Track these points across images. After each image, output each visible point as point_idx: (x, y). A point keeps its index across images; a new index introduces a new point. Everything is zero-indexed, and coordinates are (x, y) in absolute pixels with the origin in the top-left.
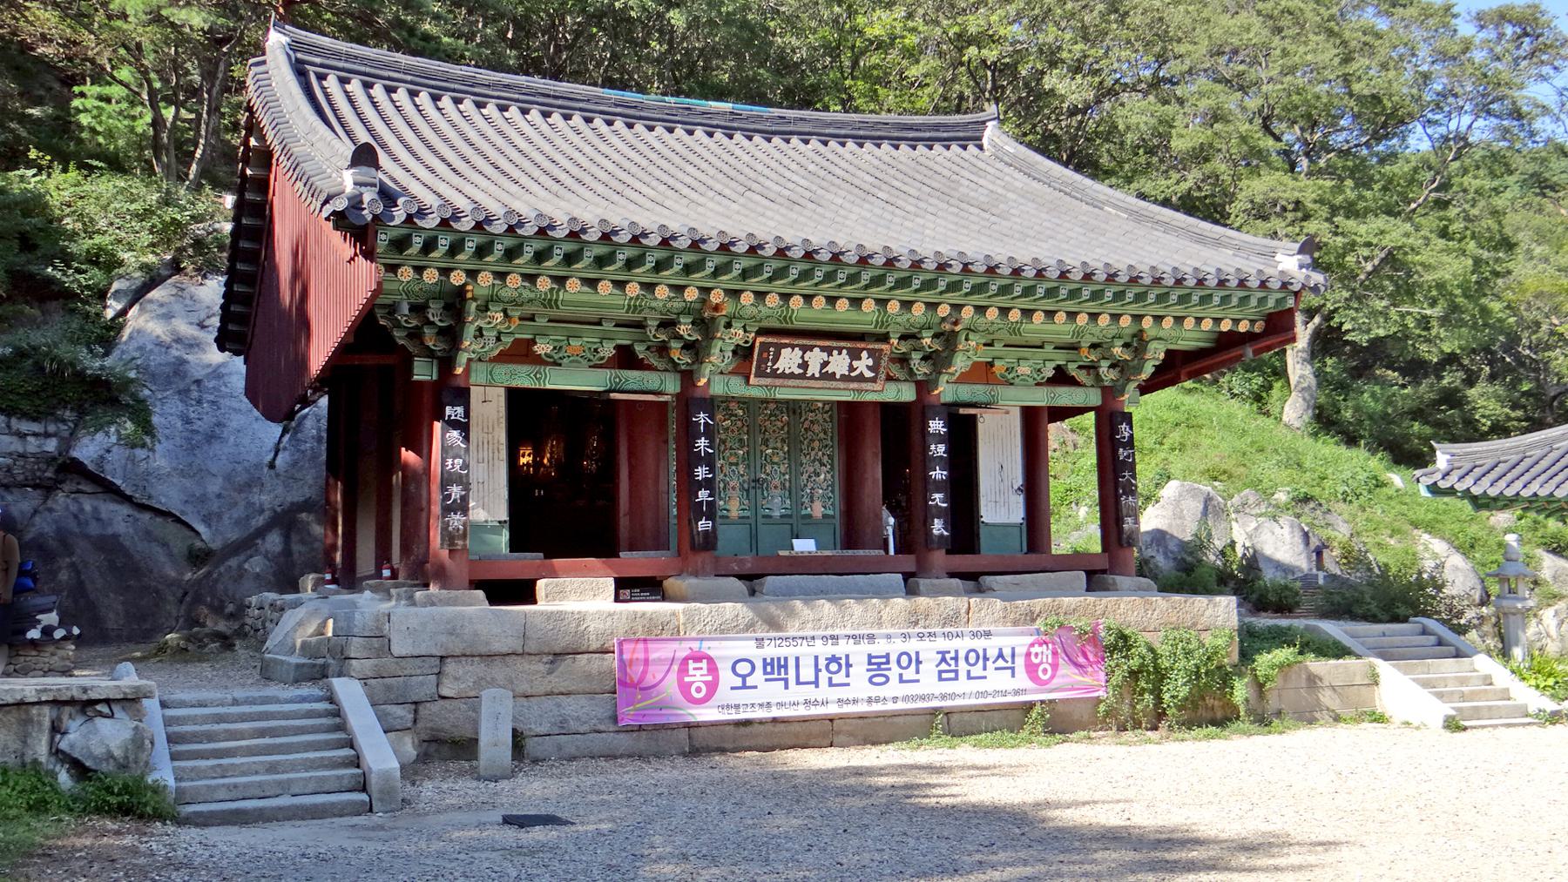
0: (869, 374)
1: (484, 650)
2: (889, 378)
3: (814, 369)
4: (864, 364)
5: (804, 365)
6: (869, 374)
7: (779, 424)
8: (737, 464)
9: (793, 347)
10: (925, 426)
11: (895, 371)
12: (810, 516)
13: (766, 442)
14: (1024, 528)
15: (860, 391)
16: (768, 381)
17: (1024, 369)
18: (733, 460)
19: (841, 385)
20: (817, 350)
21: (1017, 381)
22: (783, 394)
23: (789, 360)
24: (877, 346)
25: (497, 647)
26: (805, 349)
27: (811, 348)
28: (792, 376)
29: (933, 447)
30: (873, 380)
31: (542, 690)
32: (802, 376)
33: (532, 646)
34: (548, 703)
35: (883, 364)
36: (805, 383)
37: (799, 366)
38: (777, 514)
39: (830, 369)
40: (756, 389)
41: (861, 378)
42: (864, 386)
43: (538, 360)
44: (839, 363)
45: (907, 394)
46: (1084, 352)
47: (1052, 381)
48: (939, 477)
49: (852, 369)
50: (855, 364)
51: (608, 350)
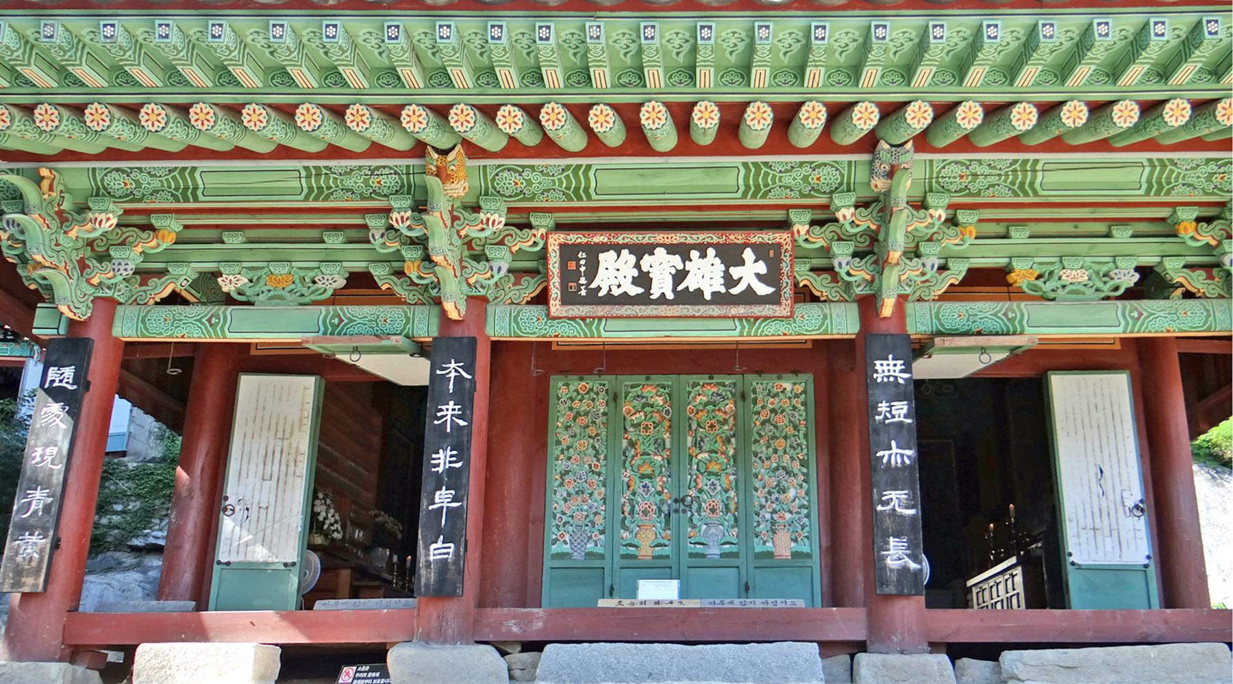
0: (763, 290)
2: (805, 295)
3: (662, 285)
4: (750, 272)
5: (643, 279)
6: (763, 290)
7: (721, 416)
8: (650, 477)
9: (618, 249)
10: (870, 369)
11: (820, 285)
12: (770, 555)
13: (698, 444)
14: (1153, 572)
16: (584, 310)
17: (1075, 274)
18: (647, 470)
19: (715, 310)
20: (660, 252)
24: (767, 237)
26: (640, 251)
27: (650, 249)
28: (625, 299)
29: (883, 407)
30: (774, 299)
32: (644, 299)
35: (785, 268)
37: (635, 282)
38: (714, 551)
39: (691, 283)
41: (749, 297)
42: (757, 310)
44: (706, 274)
45: (843, 323)
46: (1187, 230)
47: (1132, 294)
48: (896, 461)
49: (730, 281)
50: (735, 272)
51: (334, 279)
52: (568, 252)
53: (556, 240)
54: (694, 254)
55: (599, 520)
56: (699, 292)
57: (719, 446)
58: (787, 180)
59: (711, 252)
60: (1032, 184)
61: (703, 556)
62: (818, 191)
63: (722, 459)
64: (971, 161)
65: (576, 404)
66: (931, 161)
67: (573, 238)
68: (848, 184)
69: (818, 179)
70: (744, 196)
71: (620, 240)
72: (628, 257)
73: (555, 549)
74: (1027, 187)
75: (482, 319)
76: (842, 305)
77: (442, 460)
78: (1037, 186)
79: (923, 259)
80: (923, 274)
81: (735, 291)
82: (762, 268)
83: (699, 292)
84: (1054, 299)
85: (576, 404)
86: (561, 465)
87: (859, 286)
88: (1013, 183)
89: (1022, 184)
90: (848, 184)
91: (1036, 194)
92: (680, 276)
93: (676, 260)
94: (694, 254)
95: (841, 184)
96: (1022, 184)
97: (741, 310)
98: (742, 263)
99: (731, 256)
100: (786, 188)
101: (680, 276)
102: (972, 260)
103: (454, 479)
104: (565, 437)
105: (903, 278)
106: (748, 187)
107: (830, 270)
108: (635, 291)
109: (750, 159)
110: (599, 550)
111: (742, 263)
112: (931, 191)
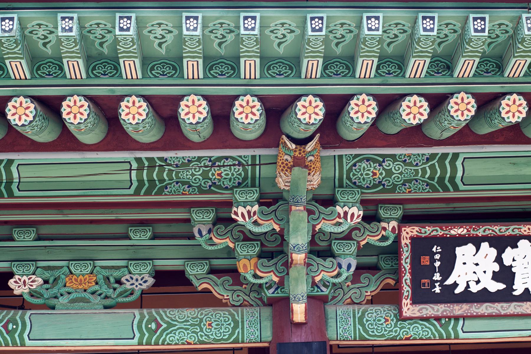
58: (185, 175)
60: (452, 179)
62: (219, 187)
64: (384, 156)
66: (340, 157)
68: (253, 178)
69: (219, 175)
70: (137, 193)
74: (446, 181)
76: (256, 311)
78: (458, 180)
79: (340, 260)
80: (339, 275)
87: (269, 288)
88: (431, 178)
89: (441, 180)
90: (253, 178)
91: (456, 189)
95: (245, 178)
96: (441, 180)
100: (184, 183)
102: (158, 262)
105: (317, 279)
106: (141, 182)
107: (233, 272)
109: (144, 155)
112: (341, 186)
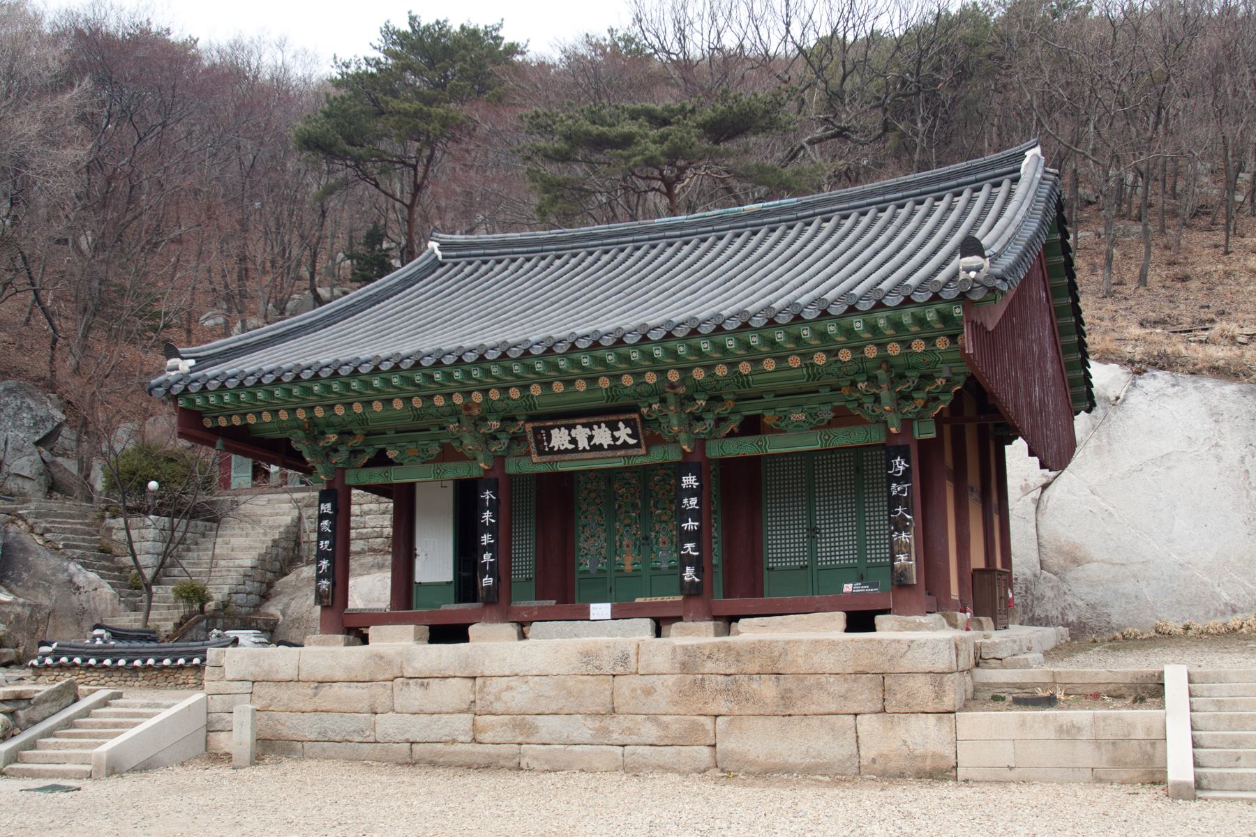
0: (632, 441)
1: (276, 678)
3: (583, 444)
4: (624, 433)
5: (573, 441)
6: (632, 441)
8: (629, 525)
15: (629, 457)
16: (549, 458)
19: (610, 454)
20: (579, 427)
21: (790, 427)
22: (562, 468)
23: (560, 439)
25: (281, 676)
26: (570, 428)
28: (566, 451)
29: (685, 501)
30: (637, 446)
31: (311, 708)
33: (303, 676)
34: (315, 717)
36: (579, 456)
37: (570, 442)
38: (665, 566)
39: (596, 441)
40: (534, 464)
41: (625, 445)
42: (630, 452)
43: (390, 463)
44: (603, 436)
49: (615, 439)
50: (616, 434)
52: (536, 431)
53: (529, 427)
54: (595, 427)
55: (603, 551)
56: (601, 445)
57: (667, 506)
59: (603, 425)
61: (659, 569)
63: (669, 513)
65: (589, 486)
67: (537, 424)
71: (559, 423)
72: (564, 431)
73: (582, 568)
75: (503, 466)
77: (486, 539)
81: (618, 443)
82: (629, 431)
83: (601, 445)
84: (781, 431)
85: (589, 486)
86: (583, 521)
92: (590, 438)
93: (587, 430)
94: (595, 427)
97: (622, 453)
98: (619, 429)
99: (613, 427)
101: (590, 438)
103: (490, 548)
104: (584, 507)
108: (571, 447)
110: (604, 568)
111: (619, 429)
